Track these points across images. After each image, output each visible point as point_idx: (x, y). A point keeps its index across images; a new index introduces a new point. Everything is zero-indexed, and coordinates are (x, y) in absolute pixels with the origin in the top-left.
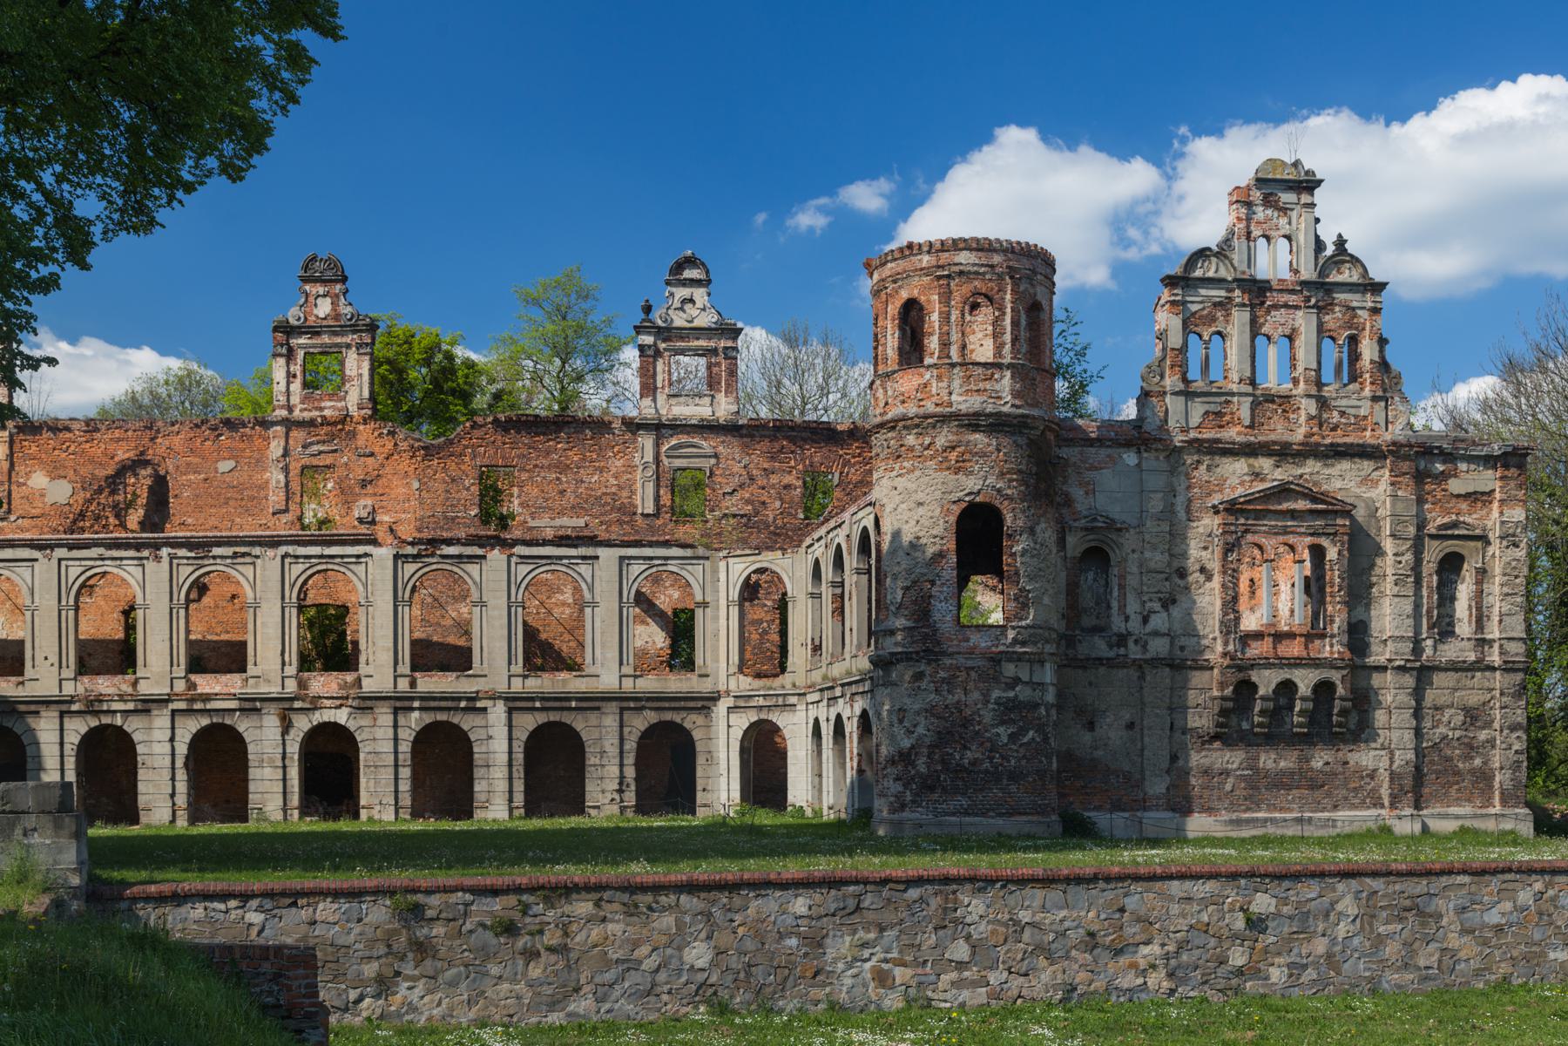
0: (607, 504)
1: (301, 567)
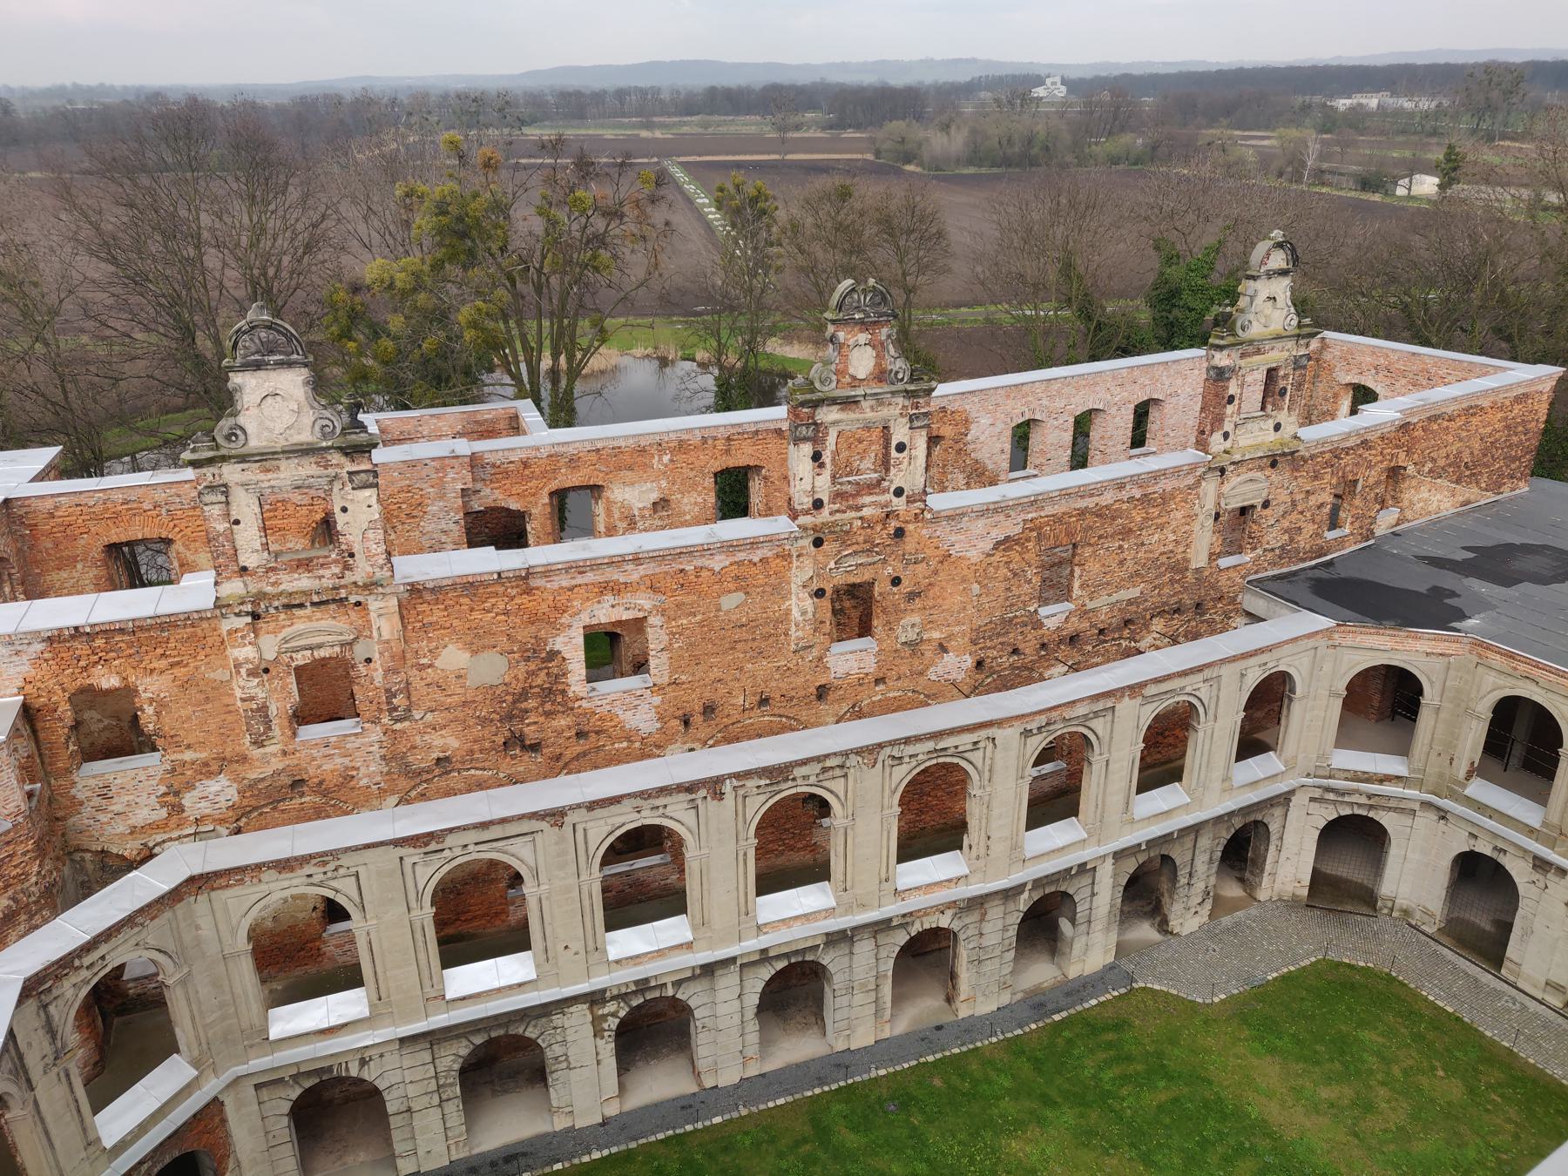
0: (1163, 564)
1: (905, 768)
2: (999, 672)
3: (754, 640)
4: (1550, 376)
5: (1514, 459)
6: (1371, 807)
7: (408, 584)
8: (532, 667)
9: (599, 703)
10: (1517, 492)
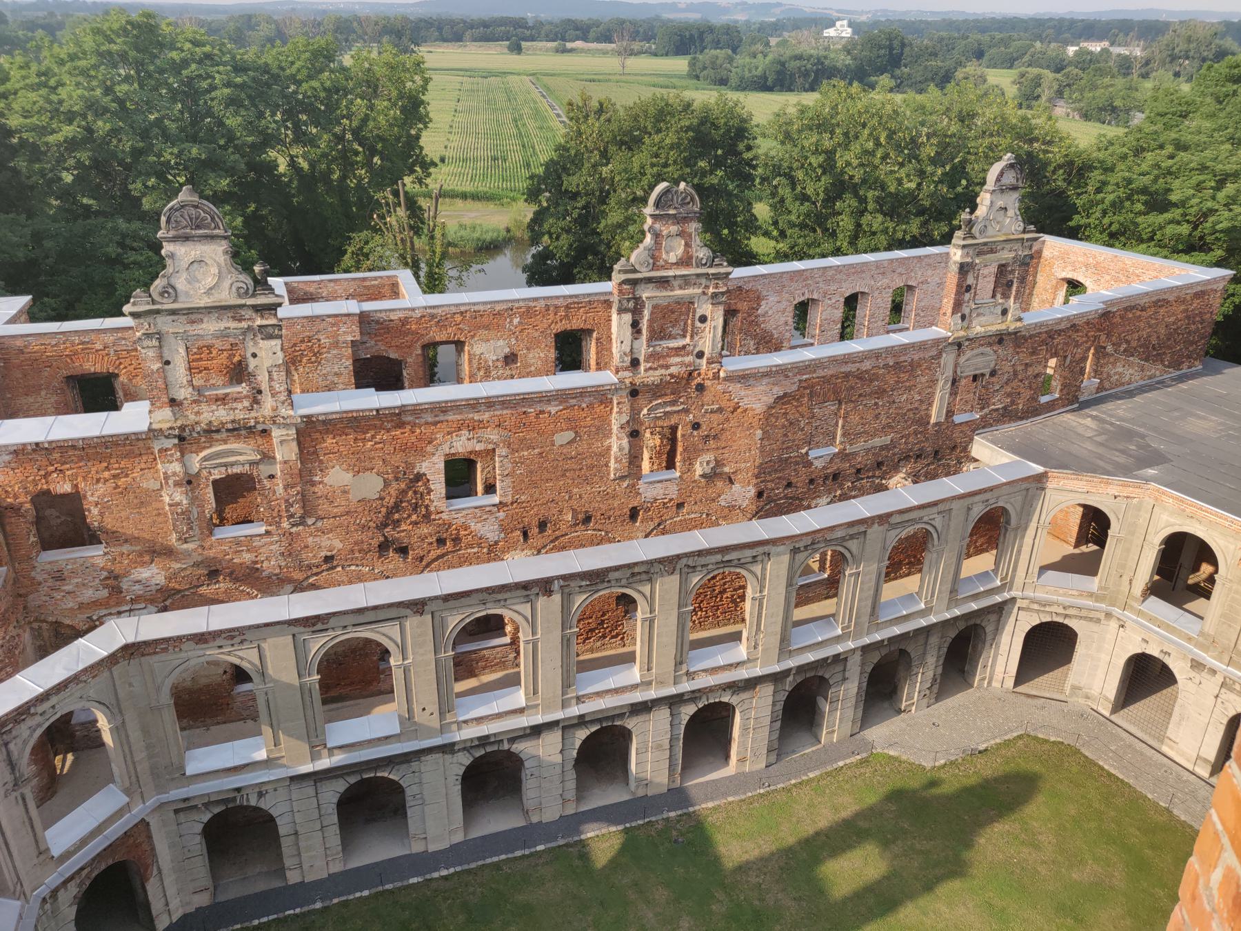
2: (776, 500)
3: (580, 469)
4: (1223, 278)
5: (1192, 343)
6: (1066, 616)
7: (305, 417)
8: (403, 486)
9: (456, 516)
10: (1194, 369)
